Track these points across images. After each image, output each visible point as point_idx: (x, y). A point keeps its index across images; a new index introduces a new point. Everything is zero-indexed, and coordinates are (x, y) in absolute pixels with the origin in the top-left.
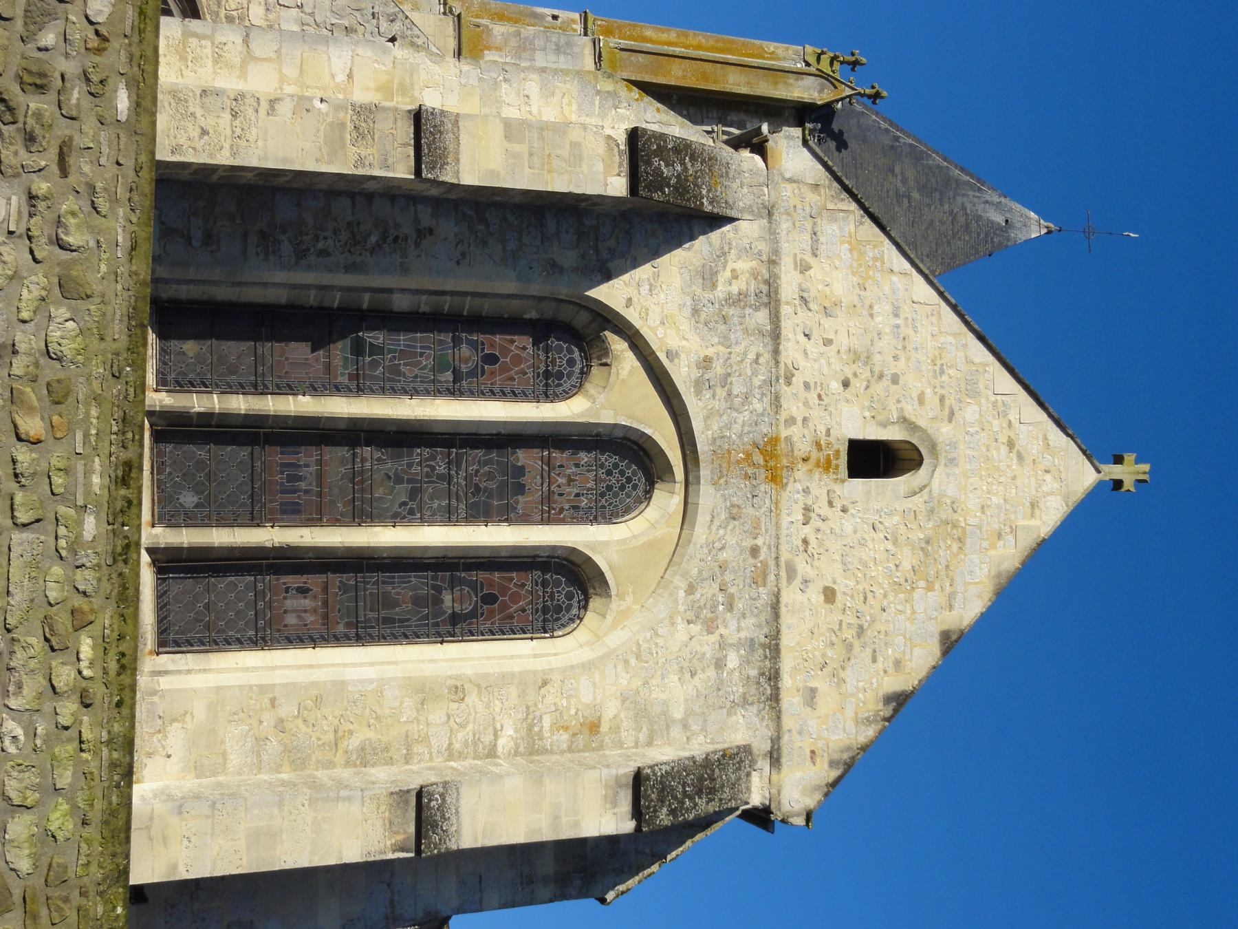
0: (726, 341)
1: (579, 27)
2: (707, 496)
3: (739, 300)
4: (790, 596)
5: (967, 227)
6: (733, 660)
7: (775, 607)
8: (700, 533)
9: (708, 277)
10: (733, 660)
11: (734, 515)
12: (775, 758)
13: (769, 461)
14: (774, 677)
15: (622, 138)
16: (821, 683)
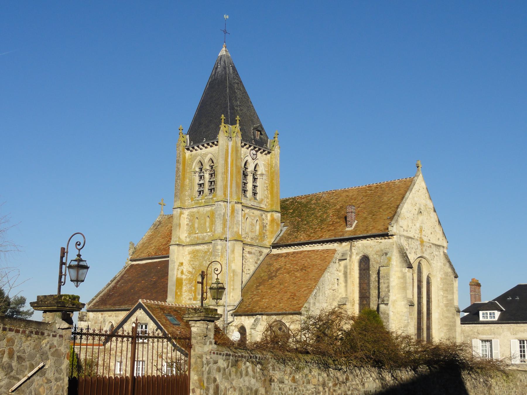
0: (412, 248)
1: (225, 203)
2: (425, 255)
3: (408, 244)
4: (431, 242)
5: (238, 84)
6: (437, 253)
7: (433, 244)
8: (427, 257)
9: (407, 249)
10: (437, 253)
11: (426, 250)
12: (443, 247)
13: (422, 243)
14: (439, 246)
15: (407, 269)
16: (438, 236)
